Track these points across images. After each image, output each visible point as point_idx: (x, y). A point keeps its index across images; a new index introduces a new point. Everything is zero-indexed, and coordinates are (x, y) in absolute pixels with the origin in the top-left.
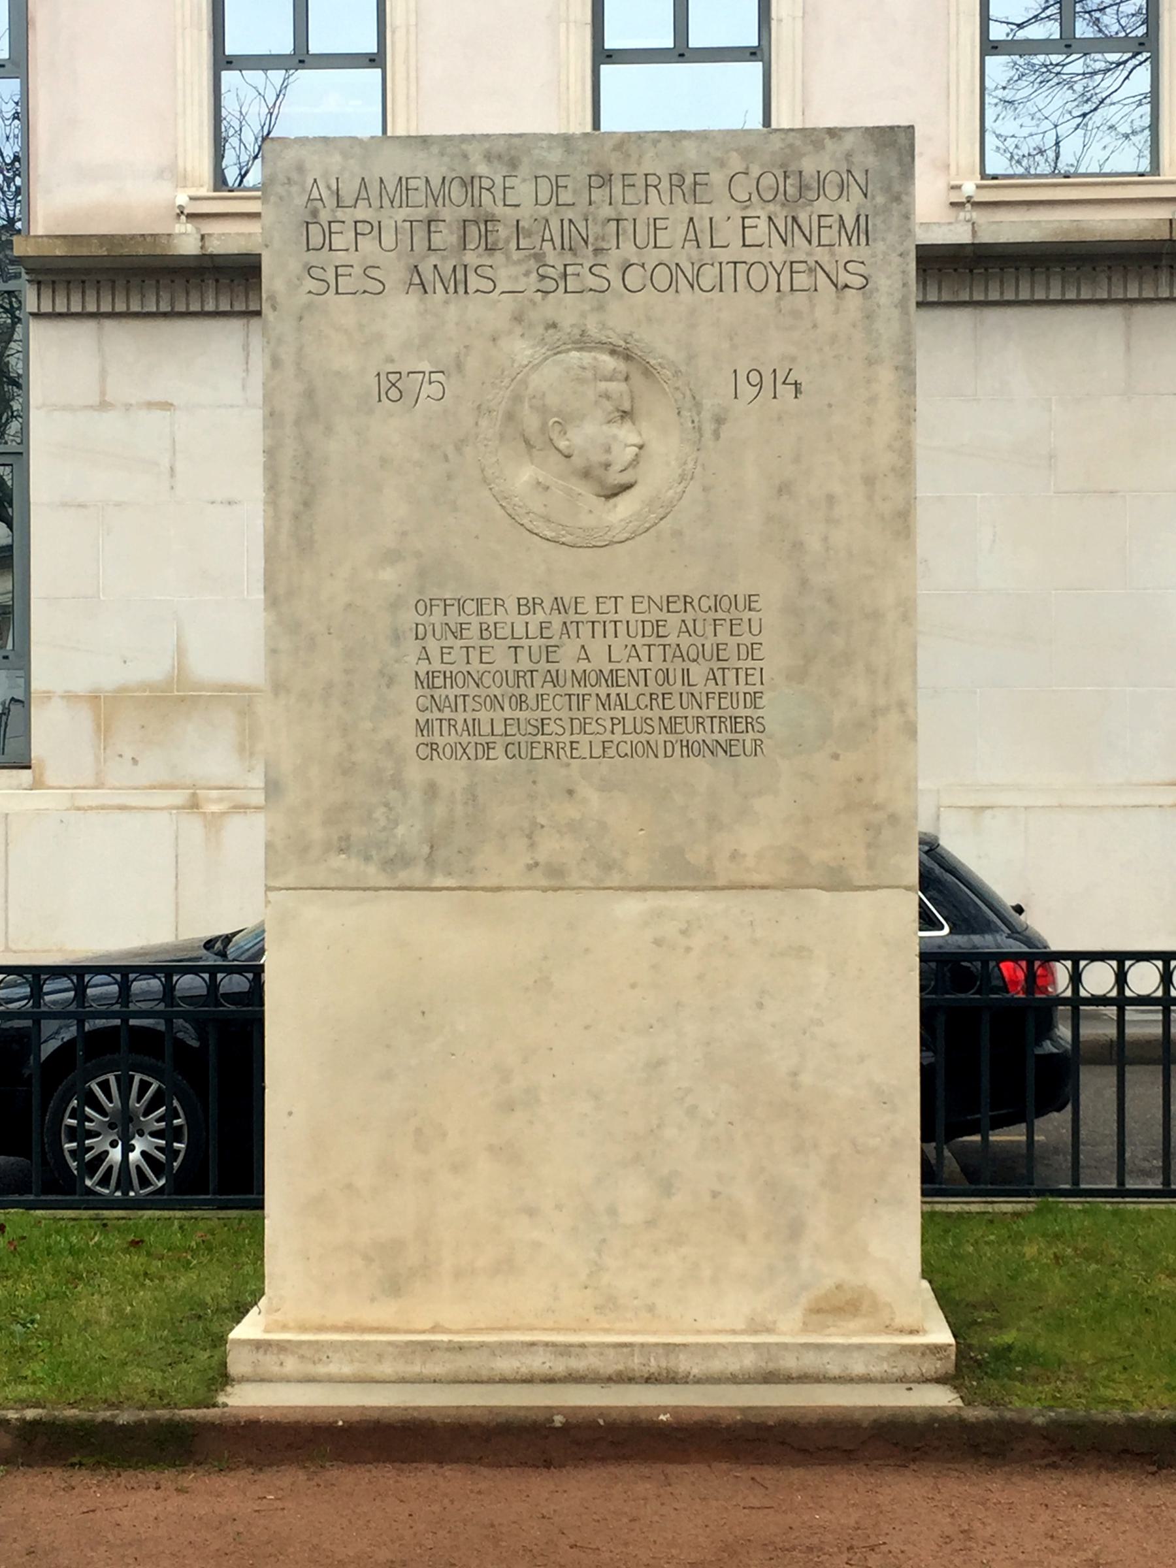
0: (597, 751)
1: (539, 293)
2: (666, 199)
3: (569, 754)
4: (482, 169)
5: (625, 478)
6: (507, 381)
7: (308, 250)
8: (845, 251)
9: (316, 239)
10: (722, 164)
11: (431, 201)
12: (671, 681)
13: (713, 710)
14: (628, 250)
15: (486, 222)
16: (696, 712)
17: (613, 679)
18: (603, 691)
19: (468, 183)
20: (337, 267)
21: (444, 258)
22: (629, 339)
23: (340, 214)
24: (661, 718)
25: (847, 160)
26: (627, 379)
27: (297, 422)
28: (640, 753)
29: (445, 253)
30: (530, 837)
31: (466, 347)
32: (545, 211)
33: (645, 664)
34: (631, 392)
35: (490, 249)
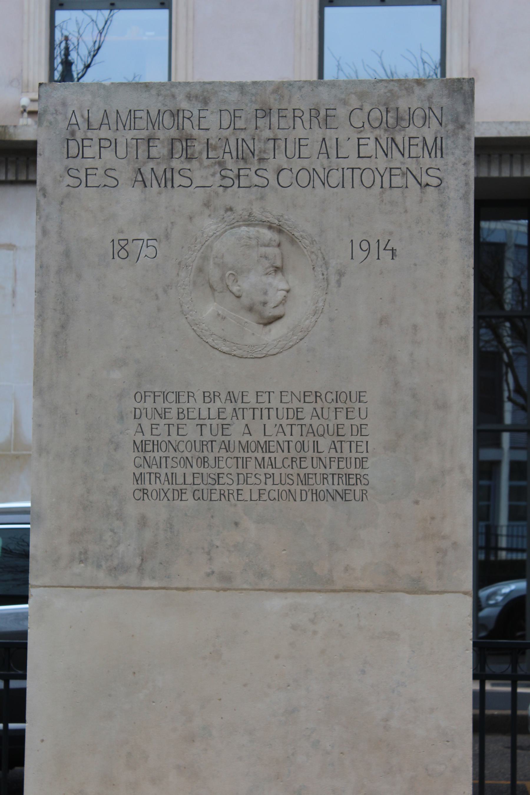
0: (255, 496)
1: (221, 188)
2: (307, 126)
3: (236, 498)
4: (184, 105)
5: (277, 312)
6: (199, 246)
7: (68, 157)
8: (426, 161)
9: (74, 151)
10: (345, 103)
11: (150, 126)
12: (306, 449)
13: (334, 469)
14: (281, 160)
15: (187, 140)
16: (322, 470)
17: (266, 447)
18: (259, 455)
19: (175, 114)
20: (86, 169)
21: (158, 164)
22: (281, 219)
23: (90, 134)
24: (298, 475)
25: (429, 100)
26: (279, 245)
27: (59, 272)
28: (284, 498)
29: (159, 160)
30: (209, 553)
31: (172, 223)
32: (226, 133)
33: (288, 438)
34: (282, 254)
35: (189, 158)
